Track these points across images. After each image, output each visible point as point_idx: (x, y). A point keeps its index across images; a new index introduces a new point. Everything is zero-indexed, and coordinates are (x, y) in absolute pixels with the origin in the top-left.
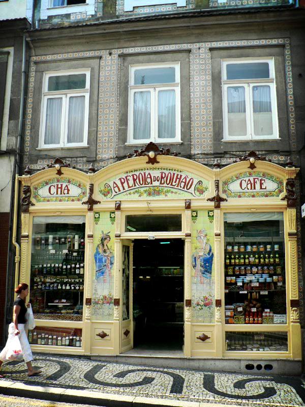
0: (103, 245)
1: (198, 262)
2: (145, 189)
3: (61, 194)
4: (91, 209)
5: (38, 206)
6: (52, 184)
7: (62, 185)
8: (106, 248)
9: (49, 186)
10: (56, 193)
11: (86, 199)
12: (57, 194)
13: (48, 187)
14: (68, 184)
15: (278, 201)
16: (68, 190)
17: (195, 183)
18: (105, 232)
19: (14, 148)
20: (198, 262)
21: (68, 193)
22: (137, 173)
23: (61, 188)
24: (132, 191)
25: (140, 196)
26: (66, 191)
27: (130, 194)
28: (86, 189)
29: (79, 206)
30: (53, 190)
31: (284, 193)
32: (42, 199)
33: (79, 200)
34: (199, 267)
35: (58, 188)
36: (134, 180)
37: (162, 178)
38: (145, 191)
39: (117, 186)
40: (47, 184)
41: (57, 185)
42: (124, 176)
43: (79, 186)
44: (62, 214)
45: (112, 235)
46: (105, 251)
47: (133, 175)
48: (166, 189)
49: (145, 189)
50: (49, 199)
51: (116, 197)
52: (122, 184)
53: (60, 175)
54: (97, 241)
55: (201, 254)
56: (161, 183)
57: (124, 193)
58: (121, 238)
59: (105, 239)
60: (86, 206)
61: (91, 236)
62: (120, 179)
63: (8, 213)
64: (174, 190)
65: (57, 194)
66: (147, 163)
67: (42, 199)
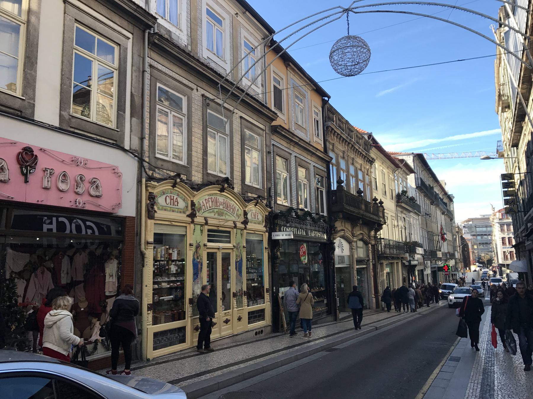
0: (197, 253)
1: (238, 264)
2: (217, 210)
3: (173, 205)
4: (193, 222)
5: (159, 214)
6: (167, 195)
7: (173, 197)
8: (198, 255)
9: (166, 195)
10: (170, 204)
11: (189, 212)
12: (171, 205)
13: (164, 197)
14: (177, 197)
15: (261, 227)
16: (178, 203)
17: (236, 210)
18: (198, 242)
19: (137, 149)
20: (238, 264)
21: (177, 205)
22: (213, 197)
23: (173, 199)
24: (211, 211)
25: (215, 215)
26: (176, 203)
27: (210, 212)
28: (187, 204)
29: (183, 217)
30: (168, 200)
31: (264, 224)
32: (161, 207)
33: (184, 213)
34: (238, 269)
35: (171, 199)
36: (212, 202)
37: (224, 204)
38: (217, 212)
39: (204, 205)
40: (164, 193)
41: (171, 196)
42: (207, 197)
43: (184, 200)
44: (174, 223)
45: (202, 244)
46: (198, 258)
47: (211, 198)
48: (225, 212)
49: (217, 210)
50: (166, 208)
51: (204, 213)
52: (207, 203)
53: (173, 188)
54: (193, 249)
55: (238, 260)
56: (223, 208)
57: (207, 212)
58: (208, 247)
59: (198, 247)
60: (189, 220)
61: (191, 245)
62: (205, 200)
63: (133, 217)
64: (229, 214)
65: (171, 205)
66: (219, 191)
67: (161, 207)
